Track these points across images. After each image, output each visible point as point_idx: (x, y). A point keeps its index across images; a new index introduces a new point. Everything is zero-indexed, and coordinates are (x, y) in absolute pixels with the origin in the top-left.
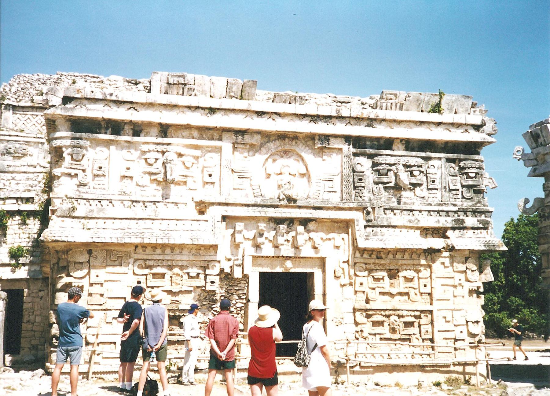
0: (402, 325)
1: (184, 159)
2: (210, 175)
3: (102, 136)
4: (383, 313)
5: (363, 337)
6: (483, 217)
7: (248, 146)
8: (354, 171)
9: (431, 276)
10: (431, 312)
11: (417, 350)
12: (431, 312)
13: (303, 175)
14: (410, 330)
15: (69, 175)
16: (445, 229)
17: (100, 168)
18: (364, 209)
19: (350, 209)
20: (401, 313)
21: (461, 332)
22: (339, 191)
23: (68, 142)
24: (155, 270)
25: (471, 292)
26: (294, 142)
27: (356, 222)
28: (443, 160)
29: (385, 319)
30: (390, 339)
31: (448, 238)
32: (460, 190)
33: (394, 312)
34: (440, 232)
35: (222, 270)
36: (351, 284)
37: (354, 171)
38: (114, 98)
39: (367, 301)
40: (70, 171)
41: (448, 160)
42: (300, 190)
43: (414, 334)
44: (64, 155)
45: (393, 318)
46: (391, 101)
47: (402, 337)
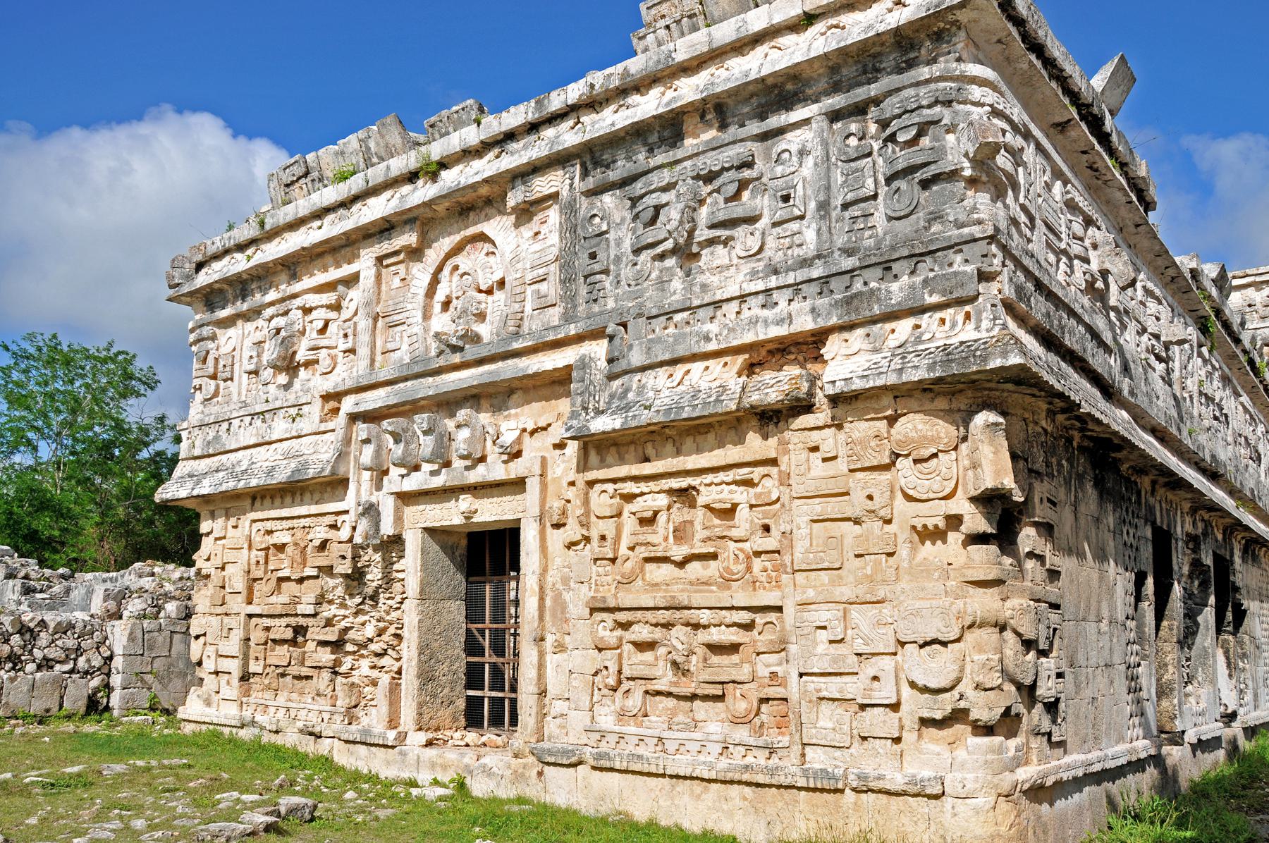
0: (701, 651)
1: (315, 314)
4: (649, 616)
5: (606, 686)
11: (742, 734)
12: (779, 609)
14: (725, 666)
16: (818, 338)
19: (579, 339)
20: (693, 615)
21: (875, 678)
28: (820, 124)
29: (658, 634)
30: (669, 694)
33: (678, 615)
41: (834, 116)
43: (734, 682)
47: (699, 691)
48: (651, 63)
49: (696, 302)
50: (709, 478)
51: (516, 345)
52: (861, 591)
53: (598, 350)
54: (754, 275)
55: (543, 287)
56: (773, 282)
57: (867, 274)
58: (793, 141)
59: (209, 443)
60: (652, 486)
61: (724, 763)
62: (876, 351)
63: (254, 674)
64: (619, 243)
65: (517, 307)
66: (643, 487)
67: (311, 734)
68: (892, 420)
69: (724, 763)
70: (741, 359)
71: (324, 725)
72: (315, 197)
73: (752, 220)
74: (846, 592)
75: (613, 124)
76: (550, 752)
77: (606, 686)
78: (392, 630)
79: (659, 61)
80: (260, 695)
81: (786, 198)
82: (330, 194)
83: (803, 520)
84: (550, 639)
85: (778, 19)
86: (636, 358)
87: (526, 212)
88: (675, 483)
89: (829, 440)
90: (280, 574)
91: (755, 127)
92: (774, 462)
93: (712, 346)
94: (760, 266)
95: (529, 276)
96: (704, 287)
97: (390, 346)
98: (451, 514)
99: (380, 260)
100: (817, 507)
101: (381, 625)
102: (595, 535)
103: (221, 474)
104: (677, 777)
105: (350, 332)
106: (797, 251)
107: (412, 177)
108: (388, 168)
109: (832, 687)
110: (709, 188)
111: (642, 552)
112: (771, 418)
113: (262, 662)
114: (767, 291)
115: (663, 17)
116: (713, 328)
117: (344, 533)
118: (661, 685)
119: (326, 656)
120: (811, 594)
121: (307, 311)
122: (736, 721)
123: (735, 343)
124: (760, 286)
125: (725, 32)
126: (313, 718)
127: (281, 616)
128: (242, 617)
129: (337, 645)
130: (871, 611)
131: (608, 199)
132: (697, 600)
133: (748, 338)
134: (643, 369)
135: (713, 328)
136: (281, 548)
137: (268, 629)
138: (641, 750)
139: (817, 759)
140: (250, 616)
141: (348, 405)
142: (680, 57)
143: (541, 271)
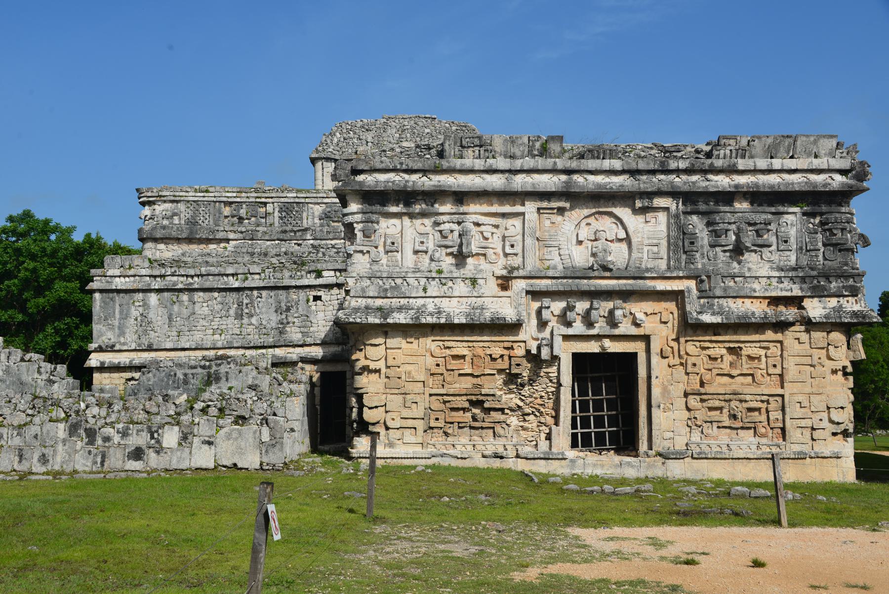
1: (483, 228)
2: (512, 246)
3: (394, 209)
4: (721, 397)
5: (696, 425)
6: (851, 282)
7: (555, 211)
8: (684, 233)
9: (782, 356)
10: (782, 396)
11: (764, 441)
12: (782, 396)
13: (620, 240)
15: (361, 252)
17: (393, 243)
18: (696, 277)
21: (821, 420)
22: (665, 257)
23: (358, 217)
24: (455, 352)
25: (834, 372)
26: (611, 203)
27: (686, 294)
29: (723, 404)
30: (730, 428)
31: (803, 308)
32: (822, 250)
33: (735, 397)
34: (796, 302)
35: (528, 352)
36: (682, 364)
37: (684, 233)
38: (404, 167)
39: (702, 384)
40: (361, 248)
42: (618, 255)
44: (356, 231)
45: (733, 404)
46: (729, 148)
48: (725, 165)
49: (747, 275)
50: (748, 345)
51: (647, 275)
52: (814, 390)
53: (692, 284)
54: (772, 268)
55: (655, 249)
56: (783, 274)
57: (820, 279)
58: (790, 218)
59: (386, 290)
60: (719, 345)
61: (760, 452)
62: (824, 308)
63: (432, 428)
64: (702, 238)
65: (640, 255)
66: (714, 345)
67: (497, 457)
68: (828, 333)
69: (760, 452)
70: (767, 301)
71: (508, 452)
72: (491, 161)
73: (770, 246)
74: (808, 390)
75: (706, 187)
76: (673, 454)
77: (696, 425)
78: (539, 401)
79: (729, 166)
80: (440, 439)
81: (786, 242)
82: (502, 163)
83: (792, 364)
84: (662, 406)
85: (785, 168)
86: (718, 292)
87: (644, 210)
88: (732, 345)
89: (804, 337)
90: (461, 372)
91: (773, 210)
92: (781, 342)
93: (757, 294)
94: (774, 266)
95: (646, 242)
96: (749, 269)
97: (546, 257)
98: (593, 347)
99: (539, 209)
100: (798, 360)
101: (531, 400)
102: (689, 362)
103: (412, 312)
104: (739, 459)
105: (515, 243)
106: (789, 263)
107: (569, 172)
108: (555, 163)
109: (803, 423)
110: (751, 228)
111: (715, 372)
112: (781, 326)
113: (443, 421)
114: (780, 278)
115: (730, 145)
116: (756, 286)
117: (520, 351)
118: (727, 424)
119: (502, 417)
120: (795, 391)
121: (477, 224)
122: (763, 436)
123: (767, 295)
124: (777, 274)
125: (762, 164)
126: (501, 450)
127: (466, 395)
128: (427, 395)
129: (502, 410)
130: (818, 397)
131: (695, 218)
132: (746, 391)
133: (774, 294)
134: (719, 297)
135: (756, 286)
136: (456, 357)
137: (445, 402)
138: (718, 449)
139: (797, 448)
140: (431, 395)
141: (519, 285)
142: (740, 167)
143: (655, 241)
